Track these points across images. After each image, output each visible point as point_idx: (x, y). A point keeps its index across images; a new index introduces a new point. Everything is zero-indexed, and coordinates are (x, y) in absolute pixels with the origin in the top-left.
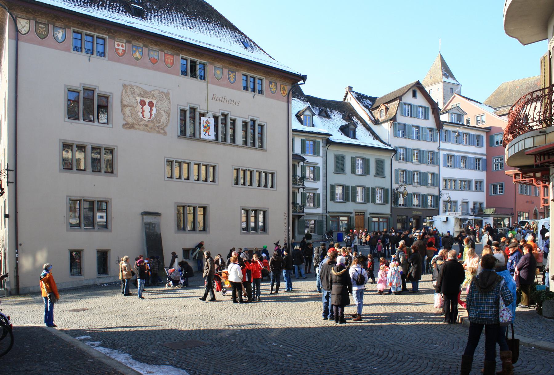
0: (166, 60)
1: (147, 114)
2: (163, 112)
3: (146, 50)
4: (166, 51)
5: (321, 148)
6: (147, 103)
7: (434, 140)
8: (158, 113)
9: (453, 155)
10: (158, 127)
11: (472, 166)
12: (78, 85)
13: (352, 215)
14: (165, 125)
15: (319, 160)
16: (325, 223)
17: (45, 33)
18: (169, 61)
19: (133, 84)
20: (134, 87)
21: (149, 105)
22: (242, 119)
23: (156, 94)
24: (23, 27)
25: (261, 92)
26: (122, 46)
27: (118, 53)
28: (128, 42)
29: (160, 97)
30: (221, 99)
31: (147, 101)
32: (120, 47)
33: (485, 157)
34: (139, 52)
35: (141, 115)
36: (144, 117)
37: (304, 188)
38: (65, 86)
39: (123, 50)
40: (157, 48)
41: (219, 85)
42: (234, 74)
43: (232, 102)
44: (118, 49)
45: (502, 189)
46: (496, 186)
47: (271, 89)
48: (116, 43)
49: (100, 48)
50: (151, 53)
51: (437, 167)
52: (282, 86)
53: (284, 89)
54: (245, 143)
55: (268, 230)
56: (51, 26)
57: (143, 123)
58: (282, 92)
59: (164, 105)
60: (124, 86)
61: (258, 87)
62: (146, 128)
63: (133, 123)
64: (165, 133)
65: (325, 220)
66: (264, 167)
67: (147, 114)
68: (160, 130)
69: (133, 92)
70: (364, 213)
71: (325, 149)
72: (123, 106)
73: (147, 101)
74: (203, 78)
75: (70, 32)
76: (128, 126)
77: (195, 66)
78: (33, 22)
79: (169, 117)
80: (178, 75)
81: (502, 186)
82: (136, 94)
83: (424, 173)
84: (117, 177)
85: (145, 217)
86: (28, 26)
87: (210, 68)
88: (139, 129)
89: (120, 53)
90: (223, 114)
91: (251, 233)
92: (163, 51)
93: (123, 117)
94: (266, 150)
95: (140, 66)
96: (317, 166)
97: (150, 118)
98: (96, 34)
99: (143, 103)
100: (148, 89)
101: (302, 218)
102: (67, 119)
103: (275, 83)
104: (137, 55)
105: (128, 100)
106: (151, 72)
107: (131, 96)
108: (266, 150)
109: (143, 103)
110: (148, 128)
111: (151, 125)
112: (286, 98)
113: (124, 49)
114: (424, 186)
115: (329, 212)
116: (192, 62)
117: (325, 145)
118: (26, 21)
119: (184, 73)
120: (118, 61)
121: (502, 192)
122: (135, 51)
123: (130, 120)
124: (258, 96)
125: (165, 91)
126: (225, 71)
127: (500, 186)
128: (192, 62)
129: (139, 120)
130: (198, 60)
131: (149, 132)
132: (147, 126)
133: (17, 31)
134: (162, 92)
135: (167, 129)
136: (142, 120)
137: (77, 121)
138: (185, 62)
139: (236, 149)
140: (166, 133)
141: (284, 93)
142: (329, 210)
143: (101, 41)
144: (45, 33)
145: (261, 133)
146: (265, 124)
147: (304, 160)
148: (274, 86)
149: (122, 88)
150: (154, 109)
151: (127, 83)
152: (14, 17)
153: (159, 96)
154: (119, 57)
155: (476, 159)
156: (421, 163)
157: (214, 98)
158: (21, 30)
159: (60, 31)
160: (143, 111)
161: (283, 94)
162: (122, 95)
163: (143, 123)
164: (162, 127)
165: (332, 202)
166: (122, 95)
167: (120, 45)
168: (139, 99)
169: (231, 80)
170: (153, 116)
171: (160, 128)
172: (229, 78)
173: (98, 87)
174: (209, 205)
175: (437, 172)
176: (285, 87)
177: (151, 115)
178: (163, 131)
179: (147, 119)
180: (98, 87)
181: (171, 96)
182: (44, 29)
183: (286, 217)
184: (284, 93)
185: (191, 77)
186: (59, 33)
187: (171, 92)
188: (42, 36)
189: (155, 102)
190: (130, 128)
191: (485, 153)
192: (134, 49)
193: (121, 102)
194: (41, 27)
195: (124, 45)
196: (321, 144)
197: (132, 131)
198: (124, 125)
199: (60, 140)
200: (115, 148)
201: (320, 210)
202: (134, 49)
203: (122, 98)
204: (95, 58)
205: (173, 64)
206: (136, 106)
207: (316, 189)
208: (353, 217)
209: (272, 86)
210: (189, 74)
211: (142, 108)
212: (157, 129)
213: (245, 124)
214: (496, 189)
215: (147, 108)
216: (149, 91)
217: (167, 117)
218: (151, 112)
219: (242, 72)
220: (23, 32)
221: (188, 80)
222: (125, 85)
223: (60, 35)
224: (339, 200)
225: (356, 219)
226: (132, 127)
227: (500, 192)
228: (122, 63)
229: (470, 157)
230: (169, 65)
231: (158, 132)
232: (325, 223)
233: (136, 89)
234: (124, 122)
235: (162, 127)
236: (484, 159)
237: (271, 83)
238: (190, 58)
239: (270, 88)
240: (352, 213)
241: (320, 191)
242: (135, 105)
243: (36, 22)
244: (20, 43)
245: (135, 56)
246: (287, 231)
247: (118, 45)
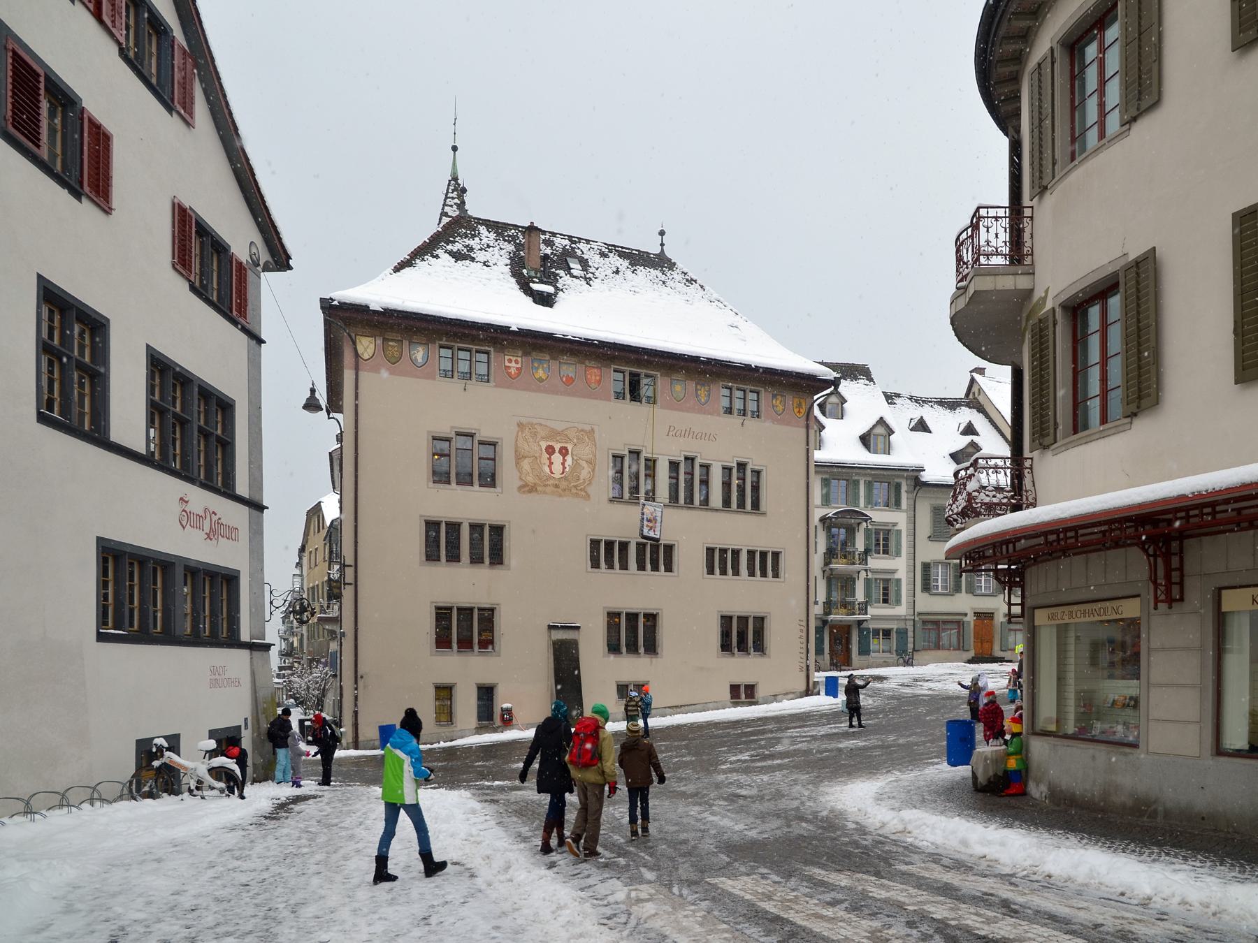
0: (589, 376)
1: (557, 467)
2: (584, 462)
3: (555, 365)
4: (587, 363)
5: (904, 496)
6: (557, 450)
8: (576, 464)
10: (575, 487)
12: (449, 431)
13: (966, 619)
15: (899, 518)
16: (910, 634)
17: (397, 354)
18: (593, 377)
19: (535, 421)
20: (536, 426)
21: (560, 452)
22: (720, 464)
23: (572, 434)
24: (366, 349)
25: (757, 414)
26: (516, 362)
27: (510, 374)
28: (526, 354)
29: (578, 439)
30: (683, 433)
31: (557, 447)
32: (513, 364)
34: (543, 368)
35: (547, 470)
36: (552, 473)
37: (866, 570)
38: (429, 432)
39: (517, 368)
40: (573, 360)
41: (681, 410)
42: (707, 388)
43: (703, 436)
44: (509, 367)
48: (507, 357)
49: (482, 369)
50: (564, 367)
52: (796, 400)
53: (800, 406)
54: (727, 502)
55: (768, 649)
56: (406, 343)
57: (551, 482)
58: (796, 410)
59: (586, 451)
60: (520, 425)
61: (752, 406)
62: (556, 489)
63: (535, 484)
64: (588, 497)
65: (910, 629)
66: (760, 545)
67: (557, 467)
68: (580, 492)
69: (535, 435)
70: (993, 613)
71: (910, 495)
72: (519, 458)
73: (557, 447)
74: (652, 400)
75: (434, 347)
76: (527, 489)
77: (639, 382)
78: (379, 341)
79: (593, 470)
80: (609, 400)
84: (509, 569)
85: (553, 632)
86: (372, 346)
87: (662, 382)
88: (545, 493)
89: (513, 373)
90: (687, 458)
91: (736, 655)
92: (583, 363)
93: (519, 474)
94: (764, 514)
95: (546, 391)
96: (896, 528)
97: (563, 473)
98: (474, 347)
99: (550, 450)
100: (559, 426)
101: (864, 625)
102: (431, 484)
103: (782, 396)
104: (541, 373)
105: (526, 447)
106: (566, 400)
107: (531, 440)
108: (764, 514)
109: (550, 450)
110: (559, 490)
111: (564, 484)
112: (803, 422)
113: (519, 366)
115: (920, 614)
116: (632, 374)
117: (912, 488)
118: (370, 339)
119: (619, 396)
120: (509, 387)
122: (537, 368)
123: (530, 479)
124: (751, 423)
125: (588, 428)
126: (691, 385)
128: (632, 374)
129: (545, 478)
130: (643, 371)
131: (560, 496)
132: (557, 486)
133: (357, 355)
134: (582, 430)
135: (590, 490)
136: (549, 478)
137: (447, 486)
138: (620, 376)
139: (709, 514)
140: (589, 496)
141: (799, 412)
142: (918, 609)
143: (484, 357)
144: (397, 354)
145: (756, 488)
146: (764, 468)
147: (867, 519)
148: (781, 401)
149: (517, 429)
150: (569, 459)
151: (524, 421)
152: (353, 335)
153: (578, 437)
154: (511, 381)
158: (363, 354)
159: (420, 349)
160: (551, 463)
162: (517, 440)
163: (551, 482)
165: (926, 595)
166: (517, 440)
167: (513, 362)
168: (544, 445)
170: (567, 470)
171: (579, 488)
172: (697, 396)
173: (479, 430)
174: (661, 610)
176: (802, 400)
177: (564, 468)
179: (557, 475)
180: (479, 430)
181: (596, 435)
182: (396, 349)
183: (802, 628)
184: (799, 412)
185: (631, 400)
186: (418, 351)
187: (596, 428)
188: (393, 361)
189: (570, 447)
190: (530, 491)
192: (536, 365)
193: (516, 451)
194: (392, 346)
195: (519, 359)
196: (904, 488)
197: (533, 496)
198: (520, 488)
199: (421, 516)
200: (506, 524)
201: (901, 610)
202: (536, 365)
203: (516, 445)
204: (473, 385)
205: (599, 382)
206: (540, 457)
207: (893, 572)
208: (969, 622)
209: (777, 402)
210: (628, 396)
211: (550, 459)
212: (574, 491)
213: (727, 470)
215: (557, 458)
216: (560, 429)
218: (563, 464)
219: (721, 383)
220: (366, 356)
221: (627, 406)
222: (522, 424)
223: (419, 354)
224: (940, 590)
225: (975, 625)
226: (532, 489)
228: (517, 389)
230: (593, 386)
231: (577, 495)
232: (910, 634)
233: (539, 428)
234: (521, 483)
237: (774, 396)
238: (628, 369)
239: (773, 406)
240: (966, 615)
241: (902, 574)
242: (537, 455)
243: (384, 339)
244: (361, 373)
245: (537, 376)
246: (804, 651)
247: (510, 361)
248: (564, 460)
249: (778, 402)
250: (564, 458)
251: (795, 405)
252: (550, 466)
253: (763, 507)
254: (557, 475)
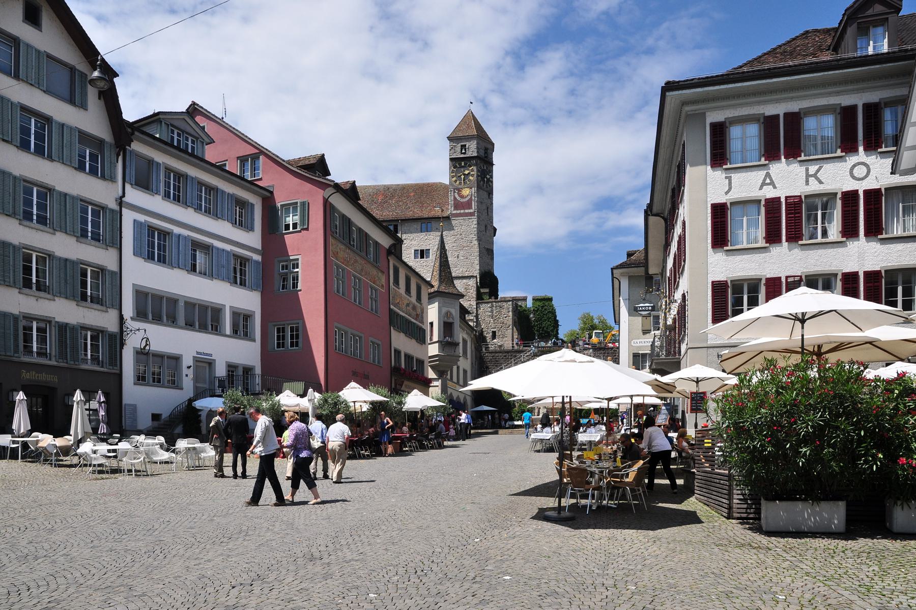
7: (107, 177)
9: (169, 233)
11: (224, 271)
33: (257, 258)
45: (297, 337)
46: (283, 328)
51: (112, 253)
81: (297, 330)
83: (66, 260)
114: (66, 298)
121: (297, 346)
127: (292, 331)
155: (236, 256)
156: (55, 230)
175: (112, 266)
191: (259, 247)
214: (283, 336)
227: (292, 345)
229: (218, 249)
236: (257, 262)
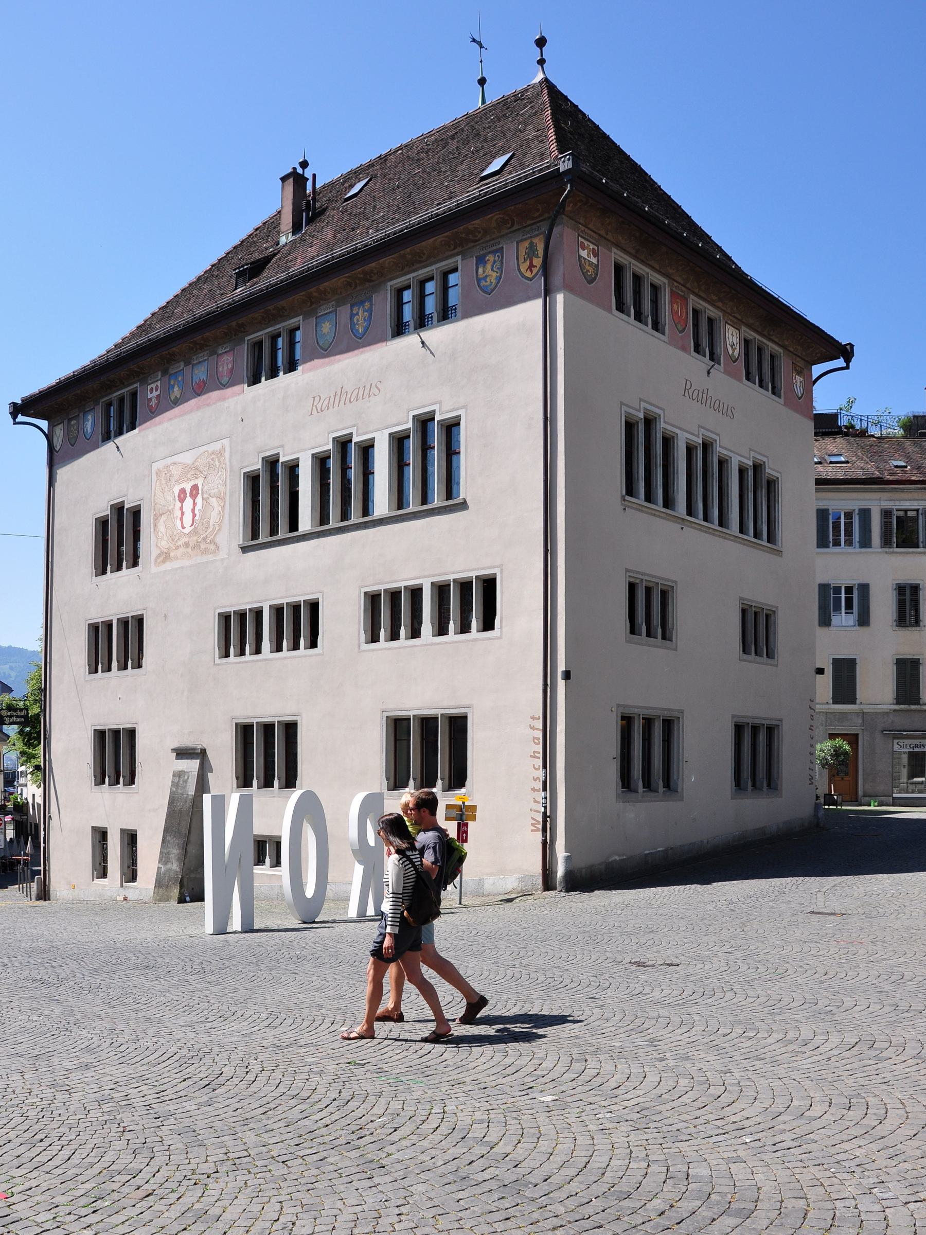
14: (217, 528)
22: (386, 433)
35: (179, 523)
36: (183, 528)
47: (483, 283)
58: (524, 267)
76: (162, 558)
82: (174, 481)
126: (344, 311)
145: (451, 452)
148: (495, 262)
150: (199, 500)
157: (314, 408)
161: (528, 274)
164: (212, 537)
169: (358, 330)
177: (194, 516)
178: (212, 547)
184: (531, 266)
212: (203, 546)
217: (220, 509)
235: (212, 537)
239: (479, 280)
248: (195, 504)
249: (489, 266)
250: (194, 501)
251: (521, 260)
252: (181, 519)
253: (465, 490)
254: (187, 531)
